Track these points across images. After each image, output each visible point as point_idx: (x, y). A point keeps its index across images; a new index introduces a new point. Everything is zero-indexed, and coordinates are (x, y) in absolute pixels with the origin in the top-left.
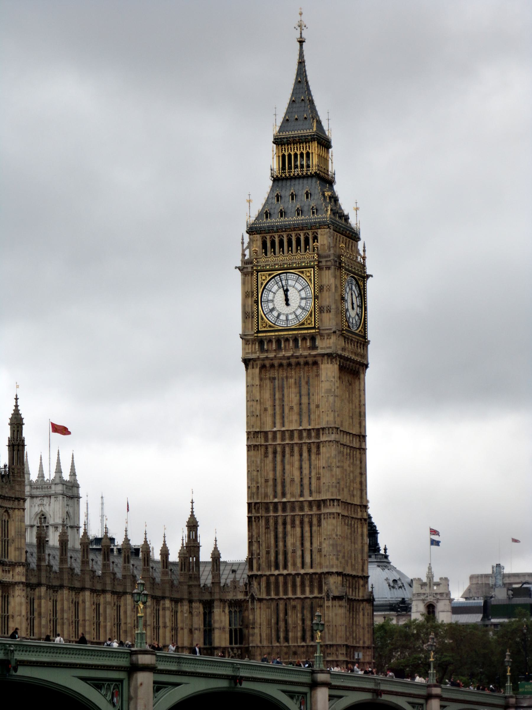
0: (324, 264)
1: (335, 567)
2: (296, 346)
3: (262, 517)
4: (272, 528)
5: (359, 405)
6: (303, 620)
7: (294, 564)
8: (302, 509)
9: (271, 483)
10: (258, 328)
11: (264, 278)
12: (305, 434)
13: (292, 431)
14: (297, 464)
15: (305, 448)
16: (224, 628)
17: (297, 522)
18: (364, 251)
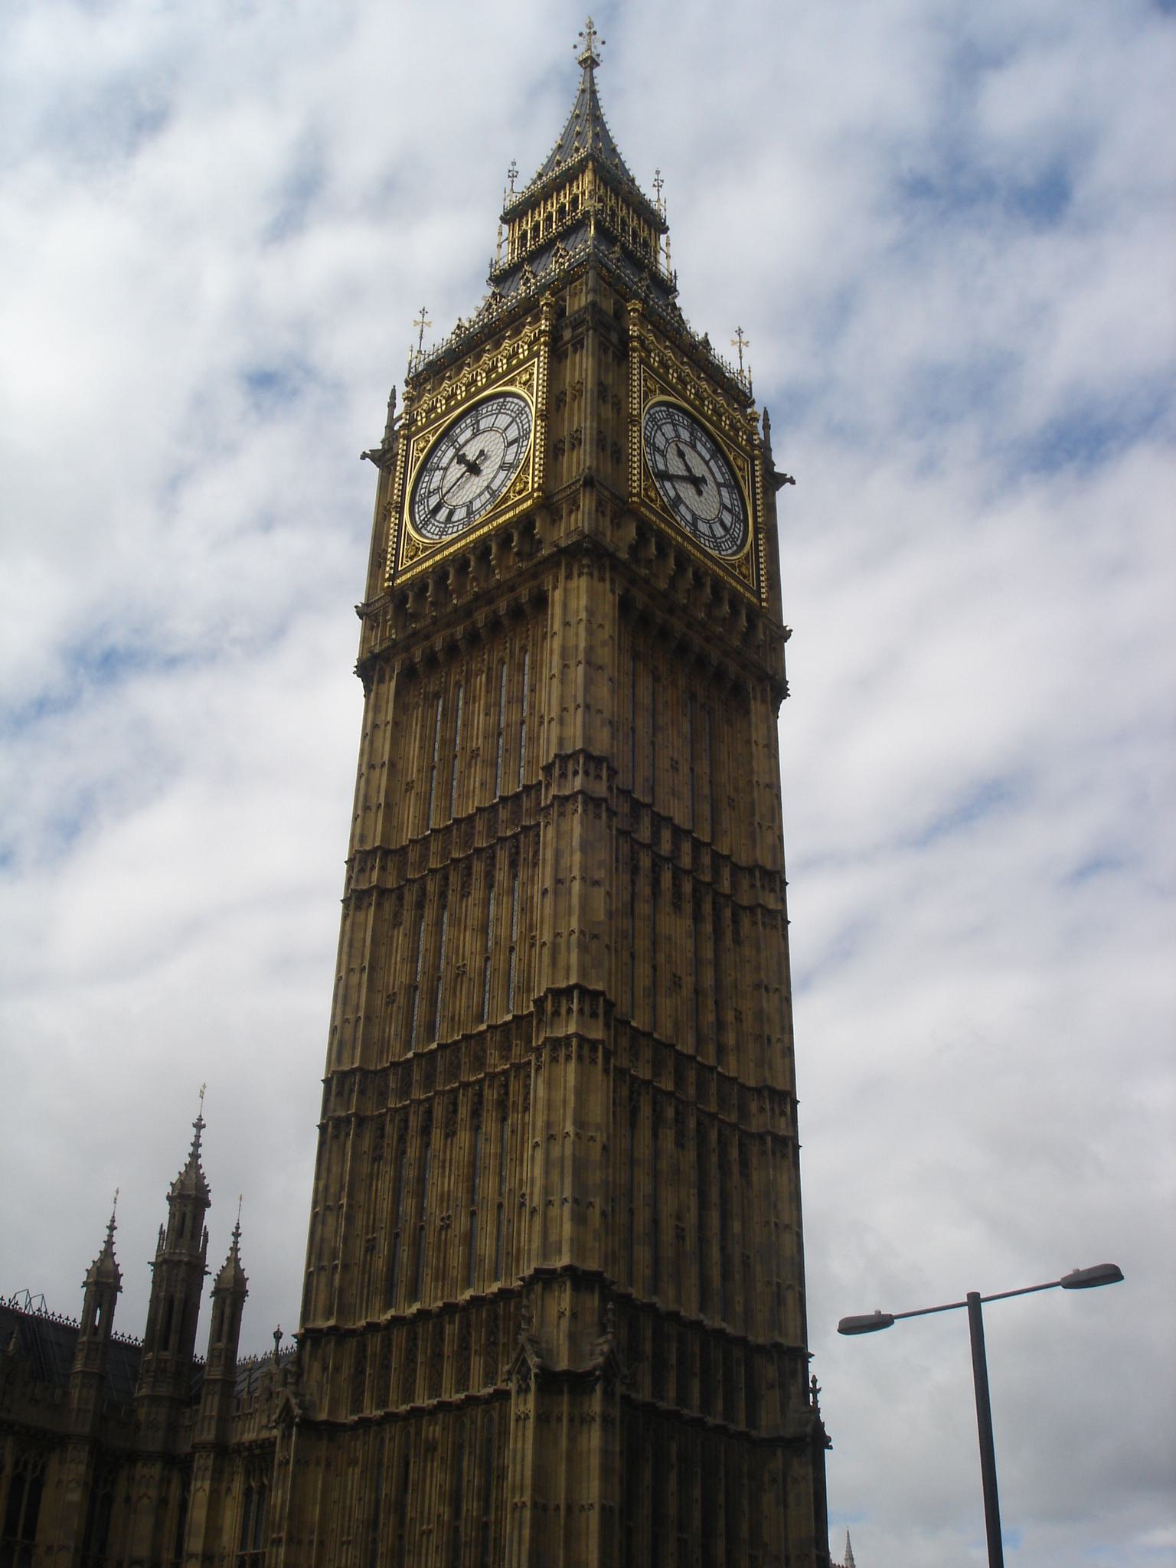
0: (567, 334)
1: (566, 1248)
2: (490, 571)
3: (361, 1121)
4: (389, 1154)
5: (750, 782)
6: (455, 1500)
7: (441, 1275)
8: (479, 1062)
9: (401, 1000)
10: (395, 568)
11: (421, 445)
12: (503, 814)
13: (470, 819)
14: (474, 914)
15: (502, 858)
16: (222, 1558)
17: (464, 1112)
18: (767, 427)
